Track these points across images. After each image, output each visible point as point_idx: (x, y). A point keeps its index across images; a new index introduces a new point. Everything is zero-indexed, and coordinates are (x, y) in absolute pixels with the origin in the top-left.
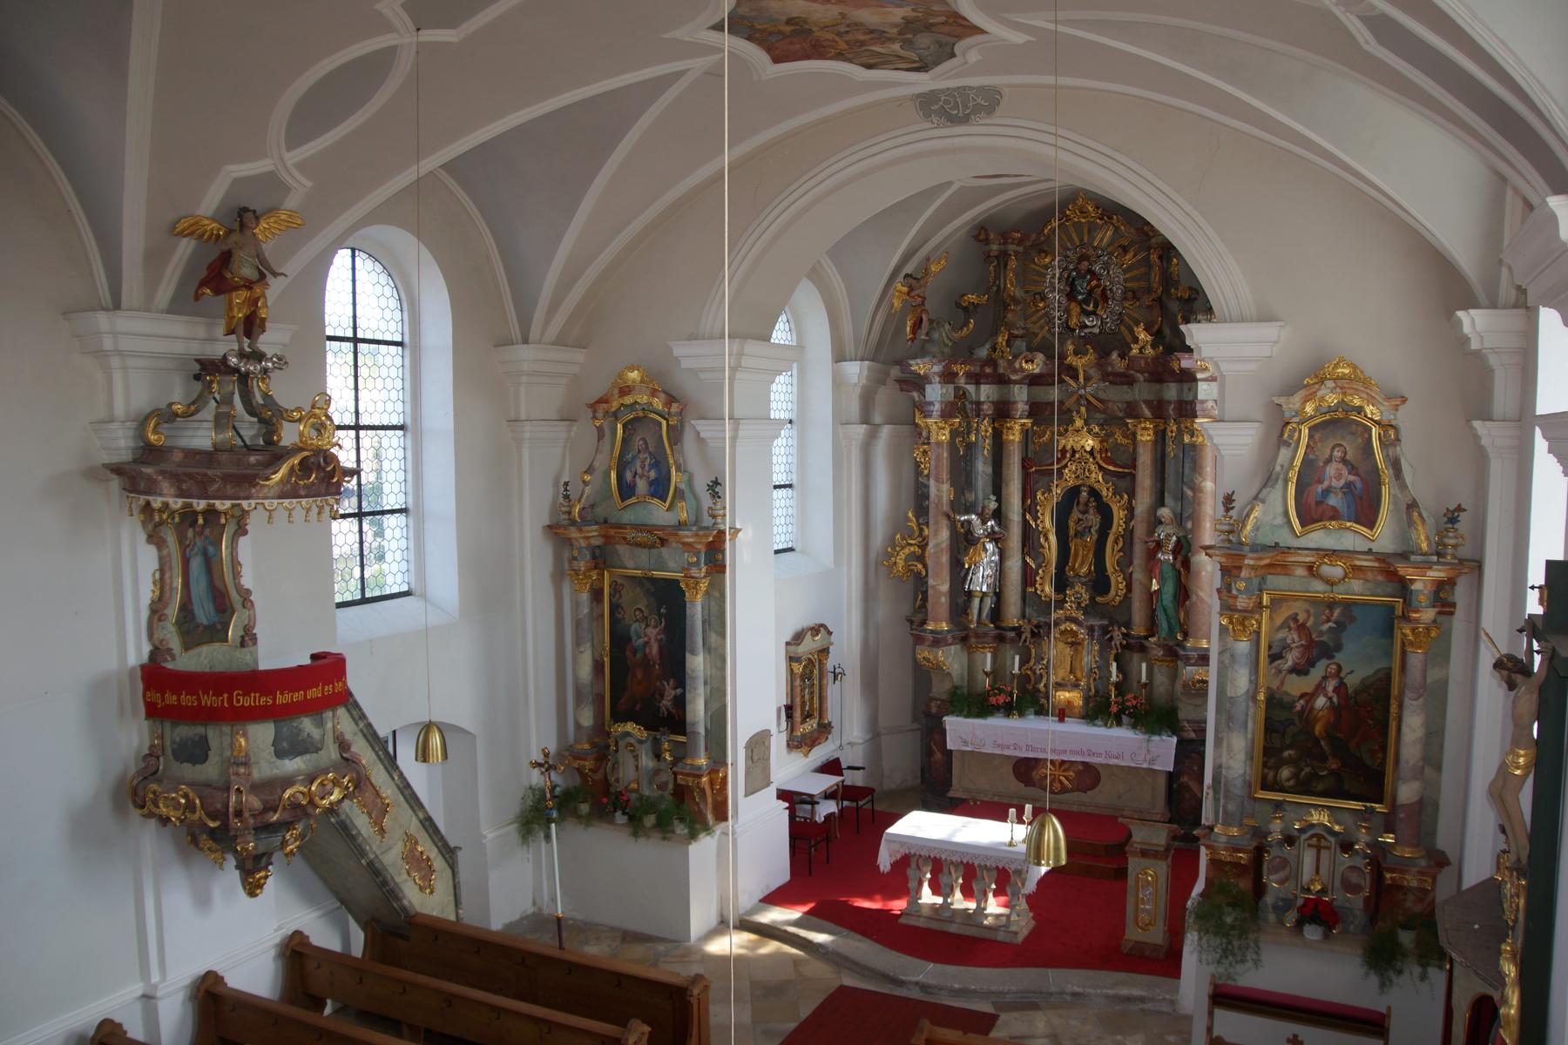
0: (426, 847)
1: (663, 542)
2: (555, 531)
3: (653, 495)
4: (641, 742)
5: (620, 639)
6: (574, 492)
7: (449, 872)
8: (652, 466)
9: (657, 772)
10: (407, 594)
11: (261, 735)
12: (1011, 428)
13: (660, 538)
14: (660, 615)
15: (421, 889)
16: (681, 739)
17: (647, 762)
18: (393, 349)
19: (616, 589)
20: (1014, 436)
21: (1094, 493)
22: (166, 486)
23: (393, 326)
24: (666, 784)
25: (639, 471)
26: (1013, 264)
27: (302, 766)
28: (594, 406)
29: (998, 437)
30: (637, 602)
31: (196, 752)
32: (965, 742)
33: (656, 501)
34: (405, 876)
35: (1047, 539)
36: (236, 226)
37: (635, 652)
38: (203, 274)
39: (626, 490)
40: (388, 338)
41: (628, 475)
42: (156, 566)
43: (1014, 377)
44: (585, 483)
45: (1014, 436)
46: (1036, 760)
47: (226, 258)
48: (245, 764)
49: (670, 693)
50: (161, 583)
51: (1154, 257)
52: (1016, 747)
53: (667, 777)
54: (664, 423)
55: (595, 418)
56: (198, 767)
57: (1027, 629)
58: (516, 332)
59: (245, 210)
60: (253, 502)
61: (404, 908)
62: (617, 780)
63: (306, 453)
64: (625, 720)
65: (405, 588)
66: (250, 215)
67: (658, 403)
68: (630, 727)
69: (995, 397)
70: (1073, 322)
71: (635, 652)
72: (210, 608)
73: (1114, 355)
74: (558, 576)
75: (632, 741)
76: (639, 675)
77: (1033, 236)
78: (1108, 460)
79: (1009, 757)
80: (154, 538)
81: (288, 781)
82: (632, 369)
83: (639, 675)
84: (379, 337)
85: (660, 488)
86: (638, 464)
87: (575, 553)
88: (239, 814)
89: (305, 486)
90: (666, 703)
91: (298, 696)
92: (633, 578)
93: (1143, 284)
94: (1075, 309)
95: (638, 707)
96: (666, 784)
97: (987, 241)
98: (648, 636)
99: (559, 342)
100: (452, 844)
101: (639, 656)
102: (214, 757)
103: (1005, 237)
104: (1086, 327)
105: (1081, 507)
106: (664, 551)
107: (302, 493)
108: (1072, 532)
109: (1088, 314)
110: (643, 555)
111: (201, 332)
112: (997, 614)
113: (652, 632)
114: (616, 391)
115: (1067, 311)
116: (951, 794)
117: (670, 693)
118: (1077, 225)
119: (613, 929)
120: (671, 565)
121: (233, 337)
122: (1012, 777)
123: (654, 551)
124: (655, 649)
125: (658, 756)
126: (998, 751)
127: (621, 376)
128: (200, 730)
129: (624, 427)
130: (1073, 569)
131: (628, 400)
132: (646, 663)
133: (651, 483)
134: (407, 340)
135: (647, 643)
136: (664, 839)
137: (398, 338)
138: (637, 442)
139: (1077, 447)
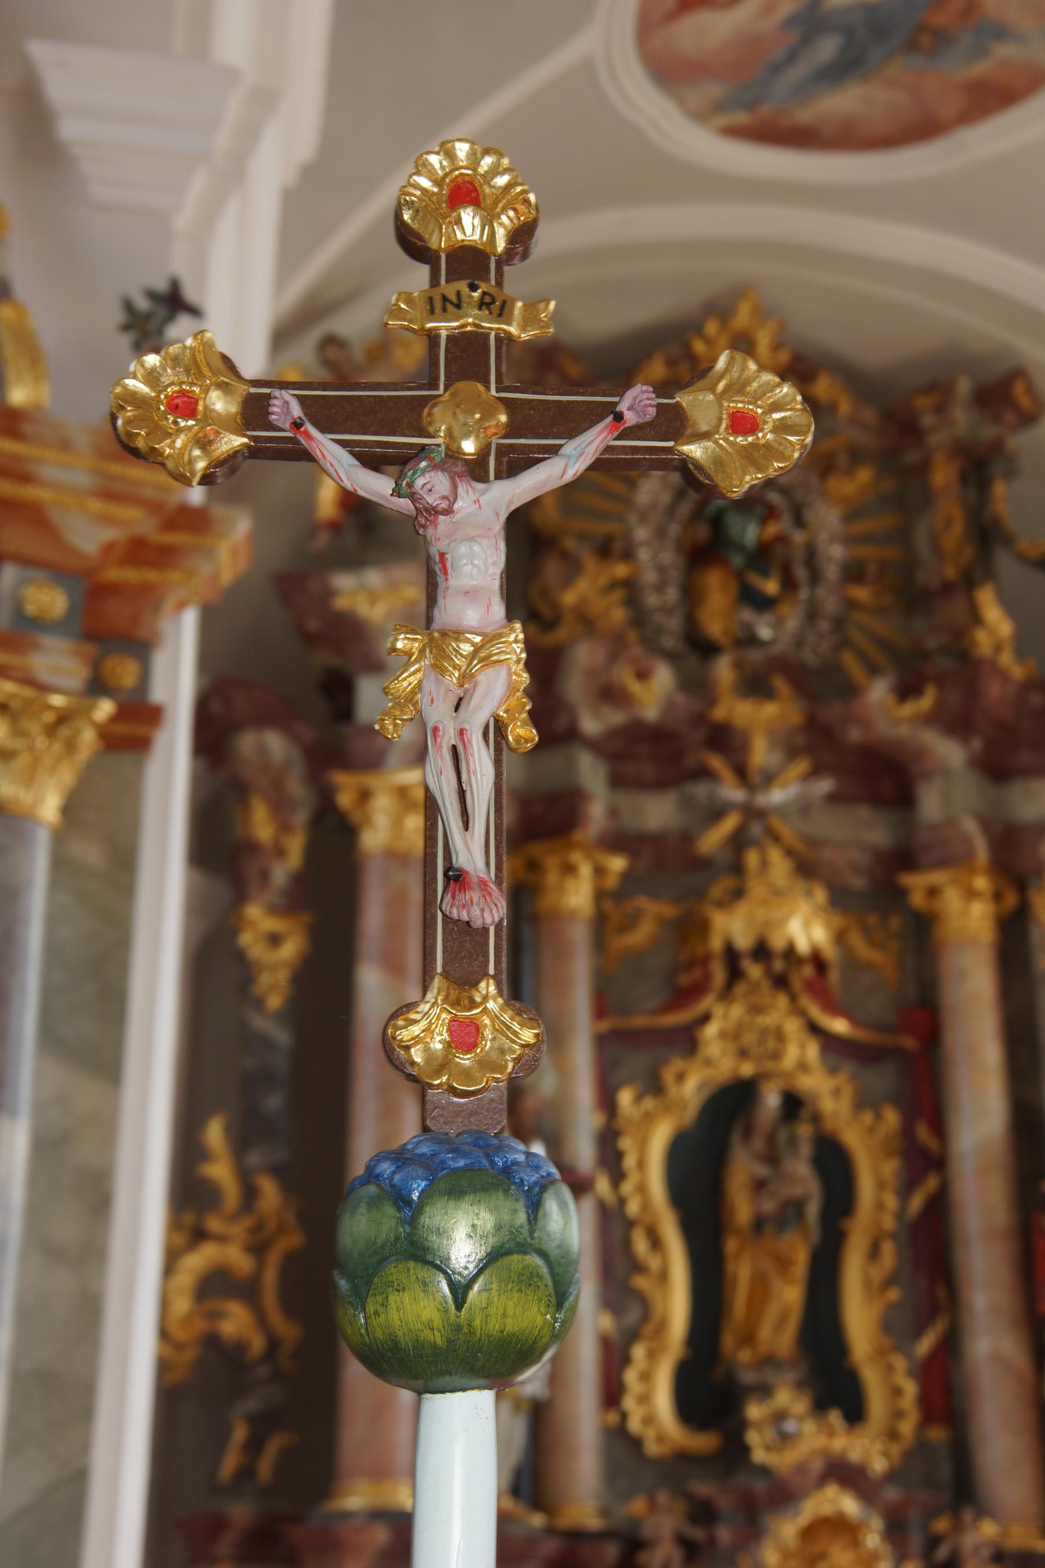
12: (570, 870)
20: (577, 896)
21: (794, 1104)
43: (590, 725)
45: (577, 896)
51: (943, 475)
70: (715, 627)
73: (878, 692)
78: (833, 1008)
94: (717, 591)
104: (749, 640)
105: (758, 1143)
109: (764, 604)
115: (691, 596)
130: (748, 1338)
139: (778, 943)
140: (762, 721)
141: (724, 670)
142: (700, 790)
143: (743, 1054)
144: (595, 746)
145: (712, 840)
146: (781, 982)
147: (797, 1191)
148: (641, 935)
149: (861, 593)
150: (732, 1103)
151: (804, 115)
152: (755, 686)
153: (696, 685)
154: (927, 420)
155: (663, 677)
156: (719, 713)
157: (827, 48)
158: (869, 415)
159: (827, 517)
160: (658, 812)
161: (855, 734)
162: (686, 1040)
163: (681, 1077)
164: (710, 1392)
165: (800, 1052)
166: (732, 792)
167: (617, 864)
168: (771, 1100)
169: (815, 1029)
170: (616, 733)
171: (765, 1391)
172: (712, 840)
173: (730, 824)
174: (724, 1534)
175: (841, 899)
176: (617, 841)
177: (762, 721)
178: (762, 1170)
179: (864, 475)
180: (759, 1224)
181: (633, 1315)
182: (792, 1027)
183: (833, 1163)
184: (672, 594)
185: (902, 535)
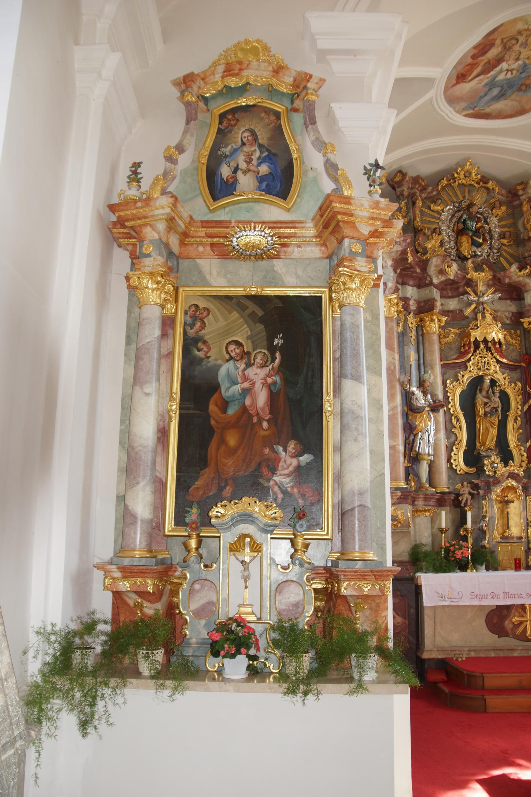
5: (198, 391)
14: (272, 349)
19: (196, 315)
20: (434, 328)
21: (493, 382)
25: (243, 165)
26: (419, 203)
28: (187, 81)
29: (420, 327)
32: (442, 597)
35: (458, 420)
37: (225, 405)
41: (225, 171)
43: (435, 281)
45: (434, 328)
46: (508, 607)
52: (493, 595)
57: (466, 490)
69: (416, 297)
70: (465, 253)
71: (225, 405)
76: (232, 440)
77: (430, 189)
78: (502, 356)
79: (481, 607)
92: (228, 298)
93: (511, 229)
97: (400, 184)
101: (231, 411)
103: (416, 180)
105: (484, 393)
108: (482, 412)
109: (479, 245)
112: (431, 481)
113: (257, 374)
114: (221, 69)
116: (425, 656)
118: (461, 185)
122: (485, 630)
123: (264, 263)
124: (262, 398)
126: (476, 602)
130: (484, 444)
132: (245, 419)
133: (261, 179)
135: (246, 392)
138: (240, 133)
139: (490, 339)
140: (480, 278)
141: (469, 264)
142: (465, 297)
143: (479, 369)
144: (436, 287)
145: (468, 312)
146: (488, 349)
147: (495, 406)
148: (450, 338)
149: (505, 241)
150: (477, 383)
151: (488, 110)
152: (478, 268)
153: (463, 269)
154: (520, 193)
155: (455, 266)
156: (469, 276)
157: (496, 91)
158: (504, 192)
159: (494, 222)
160: (453, 304)
161: (507, 280)
162: (464, 366)
163: (463, 376)
164: (473, 458)
165: (494, 367)
166: (473, 298)
167: (445, 319)
168: (487, 381)
169: (498, 361)
170: (442, 282)
171: (489, 457)
172: (468, 312)
173: (473, 307)
174: (481, 492)
175: (504, 326)
176: (444, 313)
177: (480, 278)
178: (486, 400)
179: (504, 208)
180: (485, 414)
181: (453, 439)
182: (493, 362)
183: (504, 397)
184: (453, 244)
185: (515, 225)
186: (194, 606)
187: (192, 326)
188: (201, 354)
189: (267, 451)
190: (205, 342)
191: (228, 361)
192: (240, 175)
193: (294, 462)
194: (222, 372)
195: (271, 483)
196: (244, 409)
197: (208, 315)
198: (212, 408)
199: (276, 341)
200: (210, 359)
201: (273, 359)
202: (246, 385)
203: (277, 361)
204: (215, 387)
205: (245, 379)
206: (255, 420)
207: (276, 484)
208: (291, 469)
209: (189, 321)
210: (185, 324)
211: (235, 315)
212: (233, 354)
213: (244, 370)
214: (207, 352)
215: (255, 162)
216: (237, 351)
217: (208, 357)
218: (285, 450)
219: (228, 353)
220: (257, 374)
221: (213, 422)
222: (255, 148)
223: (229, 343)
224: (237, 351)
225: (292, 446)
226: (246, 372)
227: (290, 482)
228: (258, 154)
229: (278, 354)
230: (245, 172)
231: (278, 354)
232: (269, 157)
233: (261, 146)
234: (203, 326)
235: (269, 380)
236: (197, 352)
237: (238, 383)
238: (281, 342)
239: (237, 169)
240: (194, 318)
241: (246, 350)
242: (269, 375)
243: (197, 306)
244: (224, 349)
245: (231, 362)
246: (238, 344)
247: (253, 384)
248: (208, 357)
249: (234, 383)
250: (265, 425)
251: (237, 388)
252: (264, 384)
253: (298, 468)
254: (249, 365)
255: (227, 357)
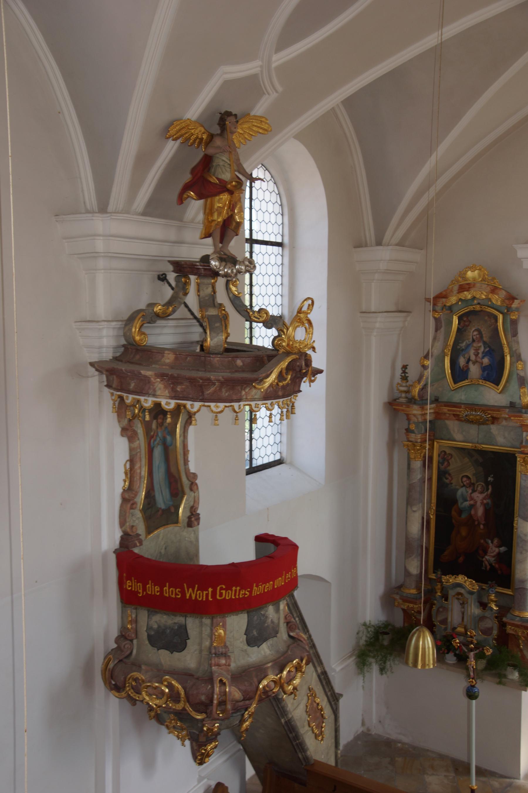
0: (322, 700)
1: (494, 420)
2: (393, 407)
3: (487, 379)
4: (471, 593)
5: (446, 503)
6: (413, 373)
7: (333, 717)
8: (485, 354)
9: (482, 618)
10: (279, 462)
11: (237, 624)
13: (490, 416)
14: (487, 483)
15: (316, 736)
16: (509, 592)
17: (474, 610)
18: (275, 248)
19: (444, 457)
22: (159, 386)
23: (277, 229)
24: (491, 629)
25: (473, 358)
27: (268, 652)
30: (462, 470)
31: (176, 641)
33: (488, 384)
34: (307, 728)
36: (216, 130)
37: (460, 512)
38: (187, 177)
39: (459, 374)
40: (273, 239)
41: (462, 361)
42: (127, 457)
44: (424, 367)
47: (207, 162)
48: (225, 655)
49: (494, 548)
50: (131, 474)
53: (491, 623)
54: (500, 317)
55: (434, 310)
56: (176, 654)
58: (370, 233)
59: (228, 114)
60: (242, 403)
61: (307, 759)
62: (444, 621)
63: (293, 357)
64: (455, 573)
65: (278, 457)
66: (232, 119)
67: (497, 299)
68: (461, 579)
72: (166, 493)
74: (392, 443)
75: (462, 591)
76: (464, 532)
80: (127, 431)
81: (259, 670)
82: (473, 268)
83: (464, 532)
84: (267, 239)
85: (494, 374)
86: (472, 352)
87: (413, 427)
88: (222, 703)
89: (283, 387)
90: (489, 558)
91: (268, 586)
92: (462, 450)
95: (461, 559)
96: (491, 629)
98: (475, 500)
99: (400, 244)
100: (337, 690)
101: (464, 516)
102: (192, 645)
106: (494, 429)
107: (280, 393)
110: (473, 430)
111: (172, 235)
113: (478, 497)
114: (456, 288)
117: (494, 548)
119: (442, 757)
120: (500, 438)
121: (209, 240)
124: (480, 511)
125: (484, 605)
127: (462, 275)
128: (179, 619)
129: (460, 318)
131: (468, 295)
132: (471, 522)
133: (484, 369)
134: (286, 240)
135: (472, 506)
136: (500, 683)
137: (279, 240)
138: (472, 333)
186: (439, 619)
187: (442, 464)
188: (447, 481)
189: (482, 541)
190: (450, 474)
191: (462, 487)
192: (471, 365)
193: (497, 550)
194: (459, 493)
195: (484, 559)
196: (470, 516)
197: (451, 458)
198: (454, 513)
199: (489, 479)
200: (453, 485)
201: (487, 490)
202: (472, 502)
203: (490, 491)
204: (455, 502)
205: (472, 499)
206: (476, 523)
207: (487, 560)
208: (495, 553)
209: (441, 460)
210: (439, 462)
211: (466, 460)
212: (465, 483)
213: (471, 493)
214: (451, 481)
215: (480, 355)
216: (468, 482)
217: (452, 483)
218: (492, 543)
219: (462, 482)
220: (478, 497)
221: (454, 521)
222: (481, 344)
223: (463, 477)
224: (468, 482)
225: (496, 541)
226: (472, 495)
227: (494, 560)
228: (482, 349)
229: (490, 487)
230: (474, 363)
231: (490, 487)
232: (489, 353)
233: (485, 343)
234: (449, 464)
235: (485, 501)
236: (445, 480)
237: (467, 501)
238: (492, 479)
239: (469, 360)
240: (444, 459)
241: (472, 482)
242: (484, 498)
243: (445, 452)
244: (460, 480)
245: (464, 488)
246: (467, 477)
247: (476, 502)
248: (452, 483)
249: (465, 500)
250: (482, 526)
251: (467, 504)
252: (482, 503)
253: (499, 554)
254: (474, 491)
255: (462, 484)
